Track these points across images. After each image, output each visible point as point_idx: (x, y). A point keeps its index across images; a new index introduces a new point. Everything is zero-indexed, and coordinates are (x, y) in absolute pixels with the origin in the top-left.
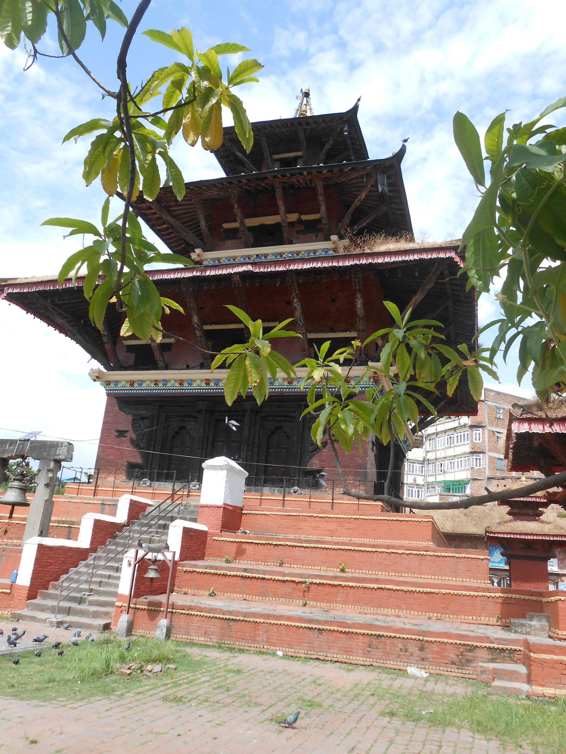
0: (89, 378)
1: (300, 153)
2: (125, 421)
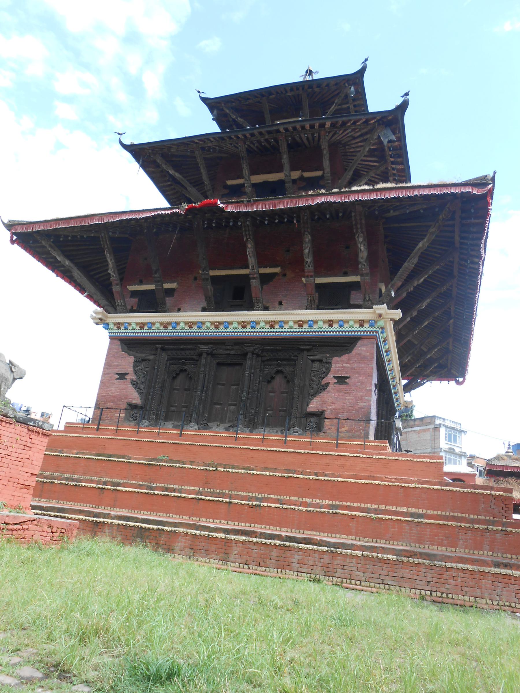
0: (92, 321)
2: (127, 363)
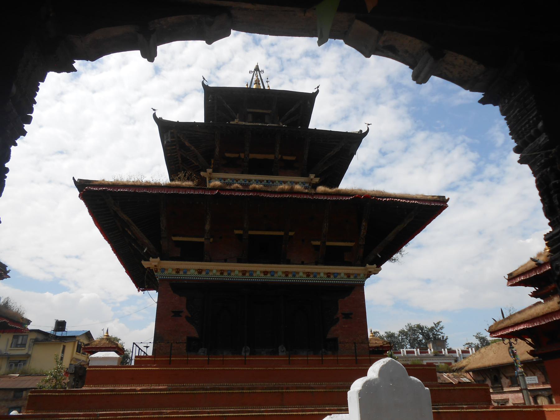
1: (269, 112)
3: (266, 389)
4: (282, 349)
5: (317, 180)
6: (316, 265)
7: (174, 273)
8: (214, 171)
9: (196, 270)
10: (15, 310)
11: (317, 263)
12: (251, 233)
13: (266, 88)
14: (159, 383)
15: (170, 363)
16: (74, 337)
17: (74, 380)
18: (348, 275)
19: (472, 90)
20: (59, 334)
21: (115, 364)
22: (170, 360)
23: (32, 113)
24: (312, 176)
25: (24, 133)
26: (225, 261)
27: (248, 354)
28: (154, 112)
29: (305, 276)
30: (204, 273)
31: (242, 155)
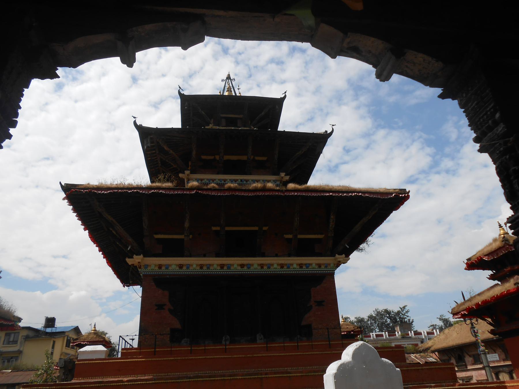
1: (241, 116)
3: (247, 375)
4: (259, 337)
5: (287, 178)
6: (289, 257)
7: (157, 268)
8: (191, 173)
9: (177, 265)
10: (6, 308)
11: (289, 255)
12: (227, 229)
13: (238, 94)
14: (145, 374)
15: (155, 353)
16: (63, 333)
17: (64, 374)
18: (320, 266)
19: (432, 85)
20: (49, 330)
21: (103, 357)
22: (155, 351)
23: (17, 117)
24: (283, 174)
25: (10, 137)
26: (205, 256)
27: (228, 343)
28: (134, 119)
29: (279, 267)
30: (184, 268)
31: (217, 157)
